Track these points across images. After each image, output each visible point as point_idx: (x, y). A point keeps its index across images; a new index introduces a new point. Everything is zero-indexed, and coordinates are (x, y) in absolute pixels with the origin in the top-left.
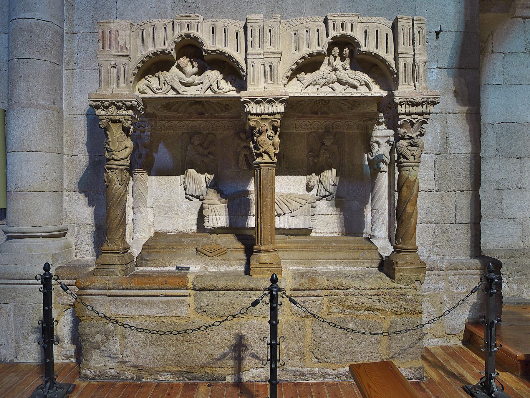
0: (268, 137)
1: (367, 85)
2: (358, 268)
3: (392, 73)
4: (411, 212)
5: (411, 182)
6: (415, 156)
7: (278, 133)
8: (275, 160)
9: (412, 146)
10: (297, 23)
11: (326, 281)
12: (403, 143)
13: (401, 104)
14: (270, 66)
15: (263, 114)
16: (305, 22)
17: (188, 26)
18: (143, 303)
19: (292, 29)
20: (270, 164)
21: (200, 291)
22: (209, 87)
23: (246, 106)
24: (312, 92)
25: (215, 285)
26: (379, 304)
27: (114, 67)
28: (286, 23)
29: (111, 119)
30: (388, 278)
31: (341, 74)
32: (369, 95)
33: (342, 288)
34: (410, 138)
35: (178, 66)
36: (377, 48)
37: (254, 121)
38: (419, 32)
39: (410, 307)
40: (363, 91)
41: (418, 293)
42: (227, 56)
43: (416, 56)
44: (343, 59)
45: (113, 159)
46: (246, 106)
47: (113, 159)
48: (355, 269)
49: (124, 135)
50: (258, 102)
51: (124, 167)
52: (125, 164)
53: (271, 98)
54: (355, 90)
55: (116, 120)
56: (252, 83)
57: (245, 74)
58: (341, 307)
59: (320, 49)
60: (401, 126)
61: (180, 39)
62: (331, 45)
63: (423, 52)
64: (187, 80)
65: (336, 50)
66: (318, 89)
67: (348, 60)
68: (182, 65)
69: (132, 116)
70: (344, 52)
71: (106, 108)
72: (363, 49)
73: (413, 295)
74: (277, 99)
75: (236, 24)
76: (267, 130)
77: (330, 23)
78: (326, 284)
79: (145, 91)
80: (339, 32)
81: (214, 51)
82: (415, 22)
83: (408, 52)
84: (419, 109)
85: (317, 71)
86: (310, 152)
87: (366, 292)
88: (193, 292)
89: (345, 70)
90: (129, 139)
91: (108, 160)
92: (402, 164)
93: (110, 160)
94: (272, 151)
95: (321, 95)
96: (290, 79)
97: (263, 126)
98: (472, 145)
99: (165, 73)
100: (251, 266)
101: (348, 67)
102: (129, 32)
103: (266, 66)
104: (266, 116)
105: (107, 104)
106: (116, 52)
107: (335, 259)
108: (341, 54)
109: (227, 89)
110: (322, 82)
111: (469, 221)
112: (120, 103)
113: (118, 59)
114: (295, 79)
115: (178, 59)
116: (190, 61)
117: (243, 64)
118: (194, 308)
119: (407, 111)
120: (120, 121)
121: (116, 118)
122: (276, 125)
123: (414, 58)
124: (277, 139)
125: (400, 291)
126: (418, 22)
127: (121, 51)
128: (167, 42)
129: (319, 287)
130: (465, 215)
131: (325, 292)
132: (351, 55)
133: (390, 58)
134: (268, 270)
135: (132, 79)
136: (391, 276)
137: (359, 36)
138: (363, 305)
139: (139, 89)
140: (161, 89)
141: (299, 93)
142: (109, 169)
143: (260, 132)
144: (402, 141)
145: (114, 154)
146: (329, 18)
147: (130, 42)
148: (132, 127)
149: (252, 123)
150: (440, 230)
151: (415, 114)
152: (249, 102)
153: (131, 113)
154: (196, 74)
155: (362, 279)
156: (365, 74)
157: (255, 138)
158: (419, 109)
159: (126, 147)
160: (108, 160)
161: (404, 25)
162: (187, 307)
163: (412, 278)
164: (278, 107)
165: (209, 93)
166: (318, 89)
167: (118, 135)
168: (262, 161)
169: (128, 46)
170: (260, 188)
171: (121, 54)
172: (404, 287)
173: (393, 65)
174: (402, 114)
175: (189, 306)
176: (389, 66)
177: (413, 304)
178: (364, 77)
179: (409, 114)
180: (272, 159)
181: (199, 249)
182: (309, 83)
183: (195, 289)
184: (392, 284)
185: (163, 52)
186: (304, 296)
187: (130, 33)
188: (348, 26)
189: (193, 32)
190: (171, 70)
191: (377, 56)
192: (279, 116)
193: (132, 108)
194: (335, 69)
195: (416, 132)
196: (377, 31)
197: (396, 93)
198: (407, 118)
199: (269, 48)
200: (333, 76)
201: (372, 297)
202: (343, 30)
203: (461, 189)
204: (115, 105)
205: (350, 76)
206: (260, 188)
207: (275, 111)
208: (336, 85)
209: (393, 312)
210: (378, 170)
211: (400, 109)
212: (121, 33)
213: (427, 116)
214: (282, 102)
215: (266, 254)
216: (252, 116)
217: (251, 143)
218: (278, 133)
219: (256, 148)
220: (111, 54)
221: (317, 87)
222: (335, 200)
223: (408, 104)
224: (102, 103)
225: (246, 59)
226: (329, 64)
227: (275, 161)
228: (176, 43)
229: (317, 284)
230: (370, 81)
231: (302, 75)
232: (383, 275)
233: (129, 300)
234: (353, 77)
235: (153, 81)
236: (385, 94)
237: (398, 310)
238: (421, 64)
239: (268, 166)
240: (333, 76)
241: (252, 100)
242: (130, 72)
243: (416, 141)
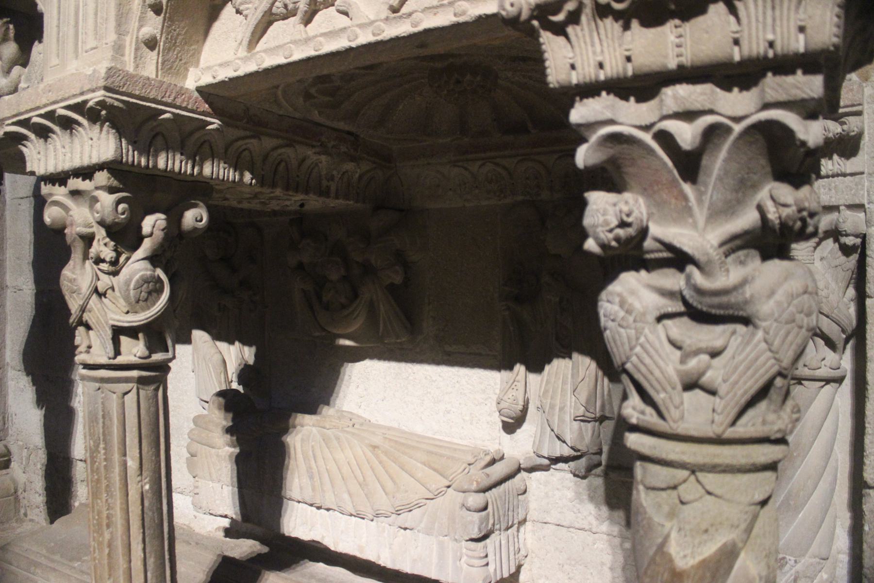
34: (679, 260)
174: (590, 90)
179: (642, 86)
198: (630, 116)
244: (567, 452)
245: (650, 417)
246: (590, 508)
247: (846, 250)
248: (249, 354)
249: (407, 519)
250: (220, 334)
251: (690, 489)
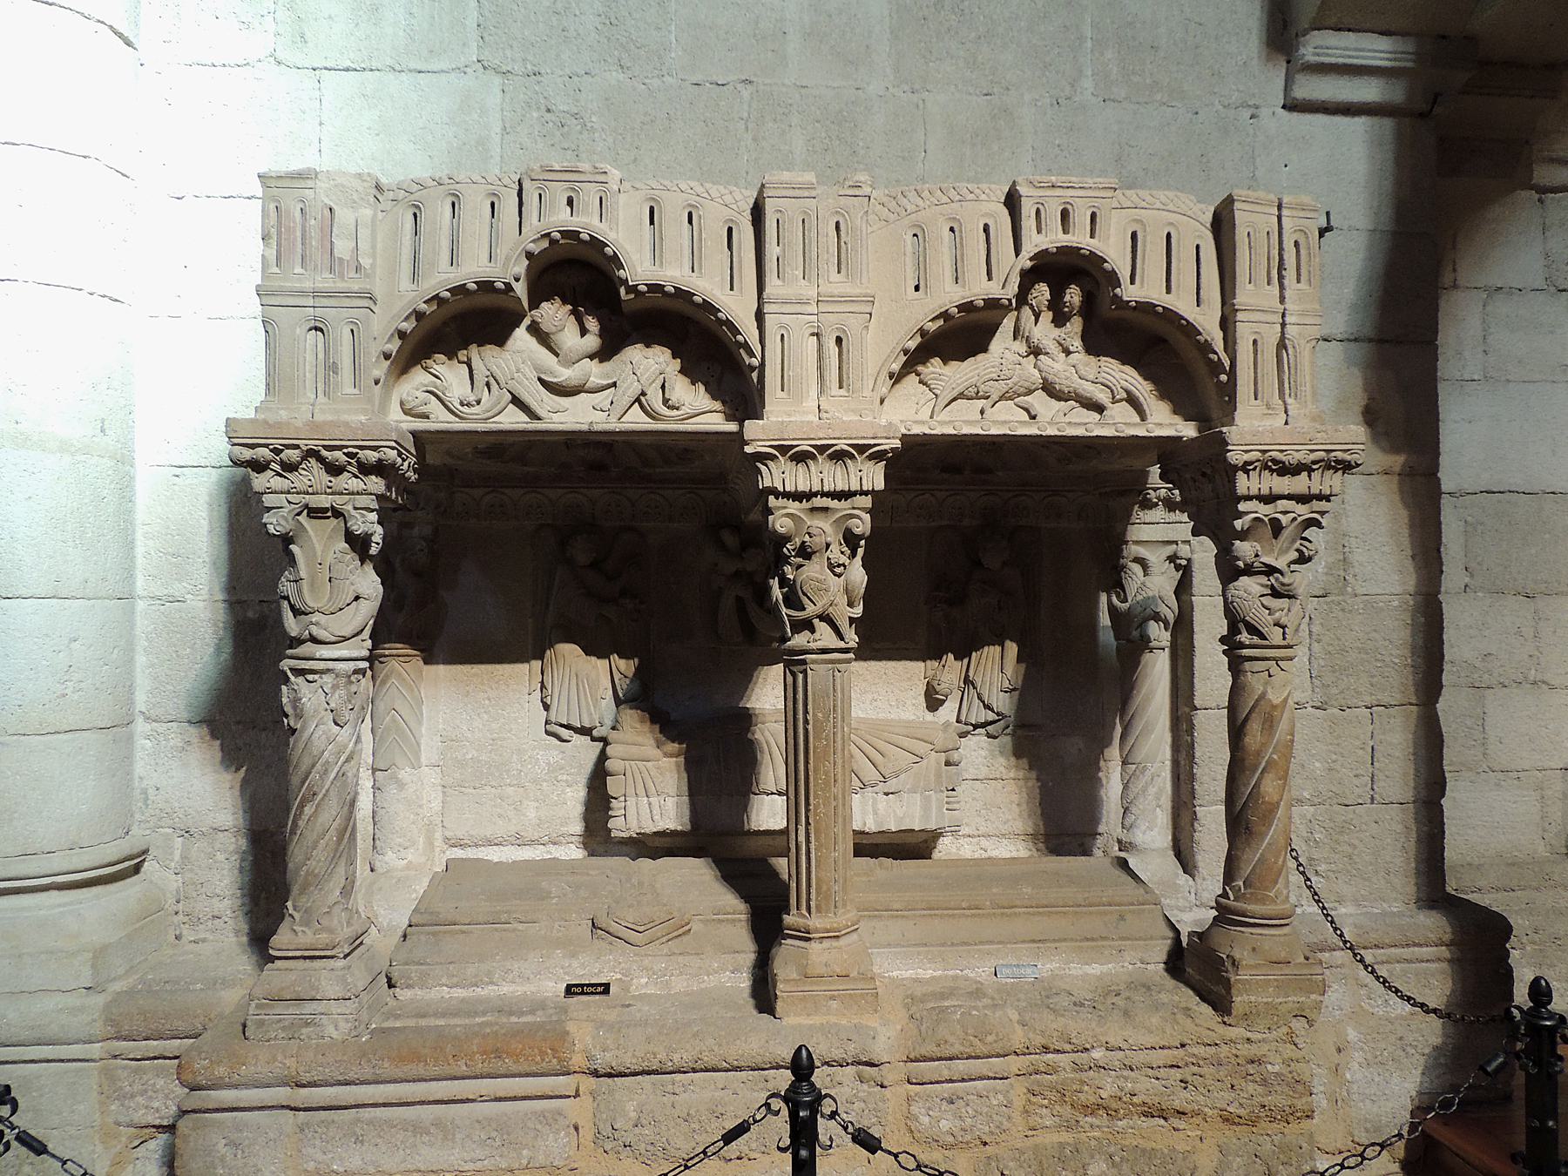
0: (831, 567)
1: (1132, 400)
2: (1105, 968)
3: (1217, 367)
4: (1275, 799)
5: (1274, 707)
6: (1283, 627)
7: (861, 551)
9: (1276, 594)
10: (920, 202)
11: (1019, 1028)
12: (1250, 587)
13: (1246, 468)
14: (839, 340)
15: (815, 494)
16: (945, 199)
17: (570, 202)
18: (417, 1128)
19: (906, 221)
21: (610, 1075)
22: (638, 400)
23: (763, 468)
24: (963, 421)
25: (662, 1056)
26: (1185, 1094)
27: (316, 329)
28: (885, 200)
29: (306, 506)
30: (1206, 1009)
31: (1055, 365)
32: (1141, 432)
33: (1068, 1047)
34: (1270, 570)
35: (535, 329)
36: (1168, 290)
38: (1296, 244)
39: (1278, 1100)
40: (1119, 422)
41: (1299, 1054)
42: (697, 305)
43: (1288, 319)
44: (1060, 320)
45: (314, 640)
46: (763, 468)
47: (314, 640)
48: (1095, 969)
49: (352, 559)
50: (801, 458)
51: (352, 666)
52: (355, 654)
53: (842, 445)
54: (1097, 416)
55: (325, 510)
56: (780, 394)
57: (755, 362)
58: (1067, 1111)
59: (994, 290)
60: (1243, 535)
61: (545, 244)
62: (1029, 278)
63: (1308, 307)
64: (564, 375)
65: (1042, 292)
66: (982, 412)
67: (1075, 325)
68: (546, 326)
69: (380, 498)
70: (1067, 298)
71: (290, 467)
72: (1130, 293)
73: (1287, 1062)
74: (861, 449)
75: (728, 199)
76: (828, 545)
77: (1027, 210)
78: (1018, 1038)
79: (423, 409)
80: (1052, 238)
81: (655, 288)
82: (1285, 212)
83: (1265, 304)
84: (1300, 484)
85: (980, 357)
87: (1142, 1057)
88: (589, 1083)
89: (1068, 352)
90: (369, 568)
91: (298, 642)
92: (1245, 652)
93: (304, 642)
95: (994, 431)
96: (896, 378)
97: (813, 531)
98: (1418, 569)
99: (490, 350)
100: (780, 986)
101: (1077, 344)
102: (368, 212)
103: (824, 340)
105: (294, 455)
106: (325, 281)
107: (1033, 941)
108: (1056, 305)
109: (696, 410)
110: (996, 389)
111: (1409, 795)
112: (338, 454)
113: (332, 302)
114: (912, 379)
115: (534, 305)
116: (574, 312)
117: (749, 332)
118: (590, 1137)
119: (1265, 491)
120: (337, 514)
121: (324, 501)
122: (857, 531)
123: (1283, 325)
124: (858, 574)
125: (1246, 1051)
126: (1295, 213)
127: (342, 276)
128: (501, 252)
129: (998, 1048)
130: (1398, 779)
131: (1014, 1064)
132: (1088, 310)
133: (1207, 321)
134: (833, 998)
135: (381, 369)
136: (1220, 1003)
137: (1115, 255)
138: (1135, 1099)
139: (402, 404)
140: (478, 402)
141: (923, 423)
142: (300, 672)
143: (805, 553)
144: (1244, 580)
145: (316, 624)
146: (1023, 190)
147: (374, 247)
148: (379, 530)
150: (1328, 824)
151: (1289, 497)
152: (773, 457)
153: (376, 484)
154: (591, 357)
155: (1126, 1013)
156: (1127, 368)
157: (788, 569)
158: (1300, 484)
159: (357, 598)
160: (298, 642)
161: (1251, 222)
162: (568, 1134)
163: (1283, 1008)
164: (863, 474)
165: (636, 420)
166: (982, 412)
167: (330, 558)
168: (813, 645)
169: (365, 262)
170: (806, 731)
171: (341, 286)
172: (1259, 1036)
173: (1219, 345)
174: (1249, 498)
175: (576, 1129)
176: (1207, 348)
177: (1286, 1089)
178: (1126, 377)
179: (1269, 499)
180: (842, 639)
181: (601, 922)
182: (955, 393)
183: (596, 1074)
184: (1221, 1029)
185: (486, 286)
186: (951, 1081)
187: (375, 215)
188: (1081, 219)
189: (587, 222)
190: (510, 342)
191: (1171, 316)
192: (867, 501)
193: (380, 469)
194: (1035, 351)
195: (1284, 551)
196: (1169, 235)
197: (1232, 433)
199: (836, 284)
200: (1030, 371)
201: (1163, 1073)
202: (1065, 231)
203: (1386, 700)
204: (321, 460)
205: (1082, 372)
206: (806, 731)
207: (855, 487)
208: (1039, 401)
209: (1227, 1120)
210: (1144, 644)
211: (1243, 484)
212: (344, 216)
213: (1323, 505)
214: (878, 457)
215: (826, 944)
216: (782, 502)
217: (775, 583)
218: (861, 551)
219: (793, 600)
220: (308, 285)
221: (981, 403)
222: (1013, 735)
223: (1266, 467)
224: (277, 451)
225: (760, 316)
226: (1016, 334)
227: (853, 644)
228: (529, 255)
229: (990, 1039)
230: (1143, 388)
231: (934, 367)
232: (1188, 997)
233: (370, 1122)
234: (1091, 377)
235: (450, 375)
236: (1188, 430)
237: (1242, 1112)
238: (1303, 342)
240: (1030, 371)
241: (783, 449)
242: (375, 349)
243: (1286, 581)
244: (991, 716)
245: (1256, 640)
246: (1002, 760)
247: (1178, 567)
248: (626, 666)
249: (892, 785)
250: (594, 649)
251: (1274, 670)
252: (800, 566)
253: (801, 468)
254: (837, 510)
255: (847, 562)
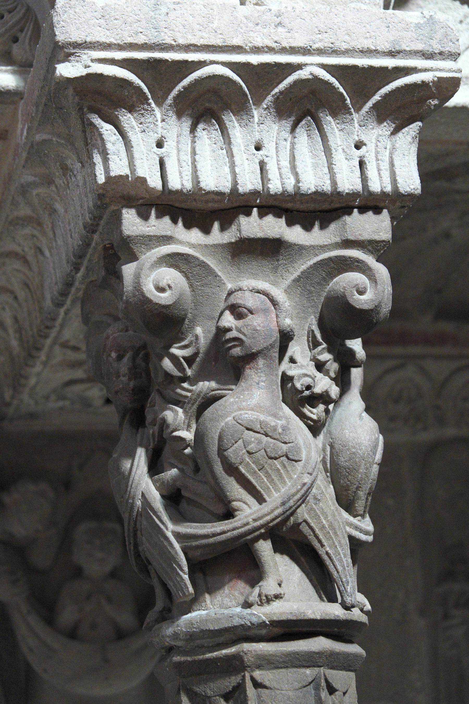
8: (357, 605)
20: (320, 644)
23: (107, 129)
37: (176, 260)
76: (286, 338)
86: (448, 575)
94: (339, 529)
104: (272, 227)
124: (357, 428)
143: (228, 361)
149: (153, 279)
157: (175, 416)
207: (349, 182)
216: (159, 225)
217: (138, 465)
239: (309, 660)
252: (209, 401)
253: (207, 137)
254: (300, 250)
255: (334, 391)
